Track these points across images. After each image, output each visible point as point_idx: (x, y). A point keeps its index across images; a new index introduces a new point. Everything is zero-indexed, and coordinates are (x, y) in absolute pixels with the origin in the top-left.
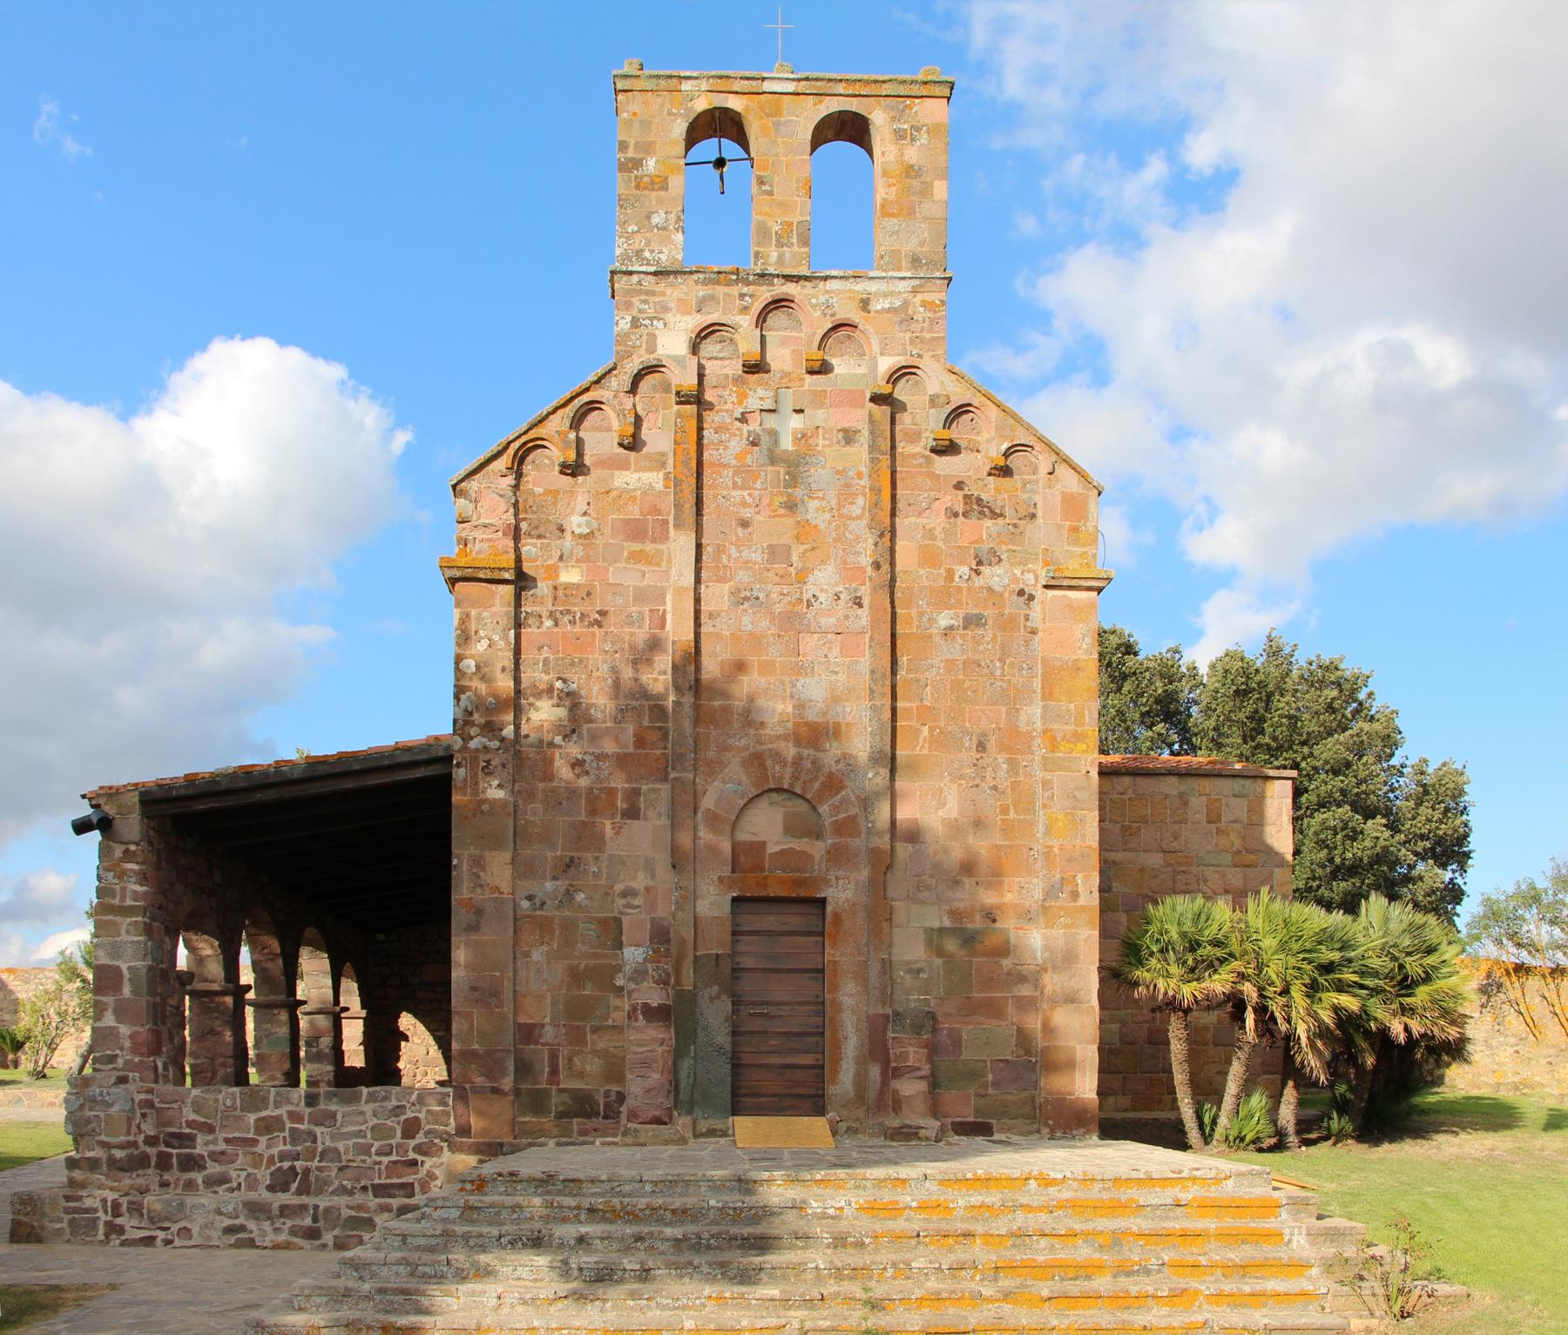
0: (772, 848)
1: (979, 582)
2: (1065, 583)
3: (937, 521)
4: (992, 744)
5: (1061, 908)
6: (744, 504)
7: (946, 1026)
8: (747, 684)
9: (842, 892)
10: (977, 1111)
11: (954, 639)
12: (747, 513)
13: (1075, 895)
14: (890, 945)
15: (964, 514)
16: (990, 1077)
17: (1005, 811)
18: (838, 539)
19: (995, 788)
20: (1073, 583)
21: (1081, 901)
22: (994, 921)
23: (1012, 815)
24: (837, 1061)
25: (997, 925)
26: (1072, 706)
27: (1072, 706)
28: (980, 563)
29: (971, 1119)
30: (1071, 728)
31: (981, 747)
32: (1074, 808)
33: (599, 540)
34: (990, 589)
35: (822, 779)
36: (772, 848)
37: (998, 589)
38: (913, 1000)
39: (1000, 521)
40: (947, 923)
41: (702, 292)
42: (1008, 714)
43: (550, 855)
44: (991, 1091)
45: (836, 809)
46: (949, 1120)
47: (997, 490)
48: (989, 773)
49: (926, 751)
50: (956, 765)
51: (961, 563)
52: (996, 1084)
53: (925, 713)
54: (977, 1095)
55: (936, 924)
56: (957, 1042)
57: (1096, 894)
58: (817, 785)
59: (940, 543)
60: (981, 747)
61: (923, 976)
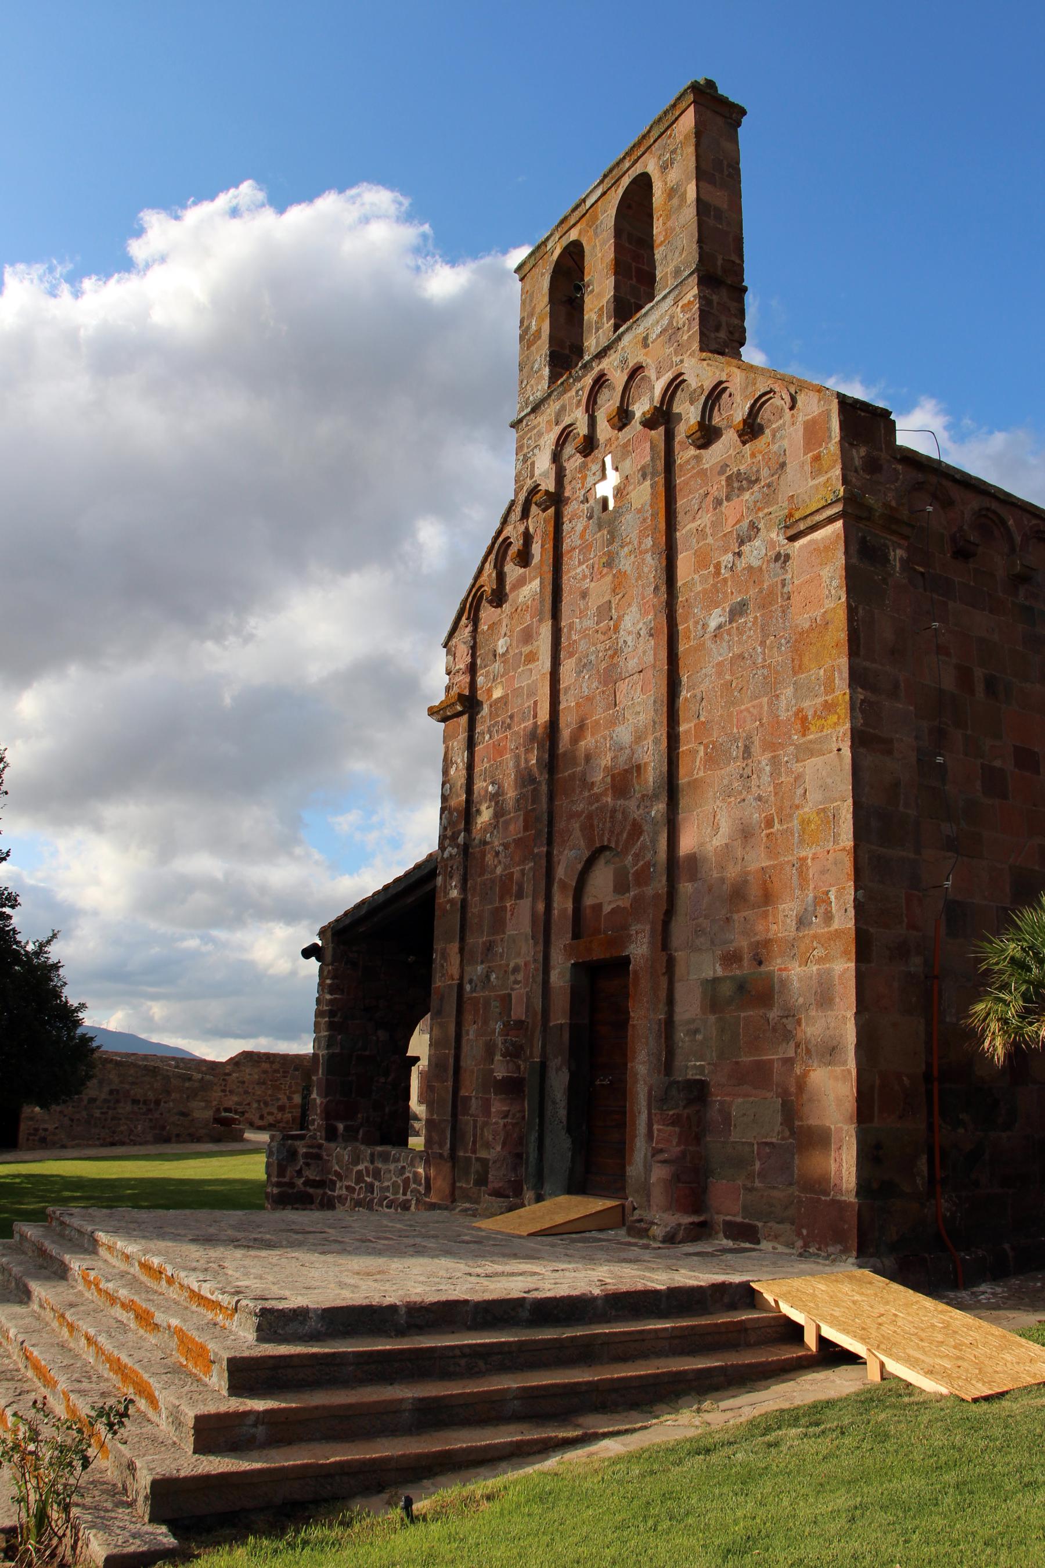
0: (607, 909)
2: (802, 526)
4: (756, 749)
5: (815, 937)
7: (717, 1098)
8: (588, 742)
9: (639, 949)
10: (745, 1208)
11: (722, 639)
13: (829, 918)
15: (728, 499)
16: (757, 1165)
17: (769, 823)
20: (809, 522)
22: (760, 963)
25: (763, 969)
28: (742, 543)
29: (739, 1219)
30: (820, 700)
34: (750, 568)
35: (628, 827)
36: (607, 909)
37: (756, 563)
39: (756, 488)
42: (770, 703)
43: (481, 941)
44: (757, 1184)
49: (701, 774)
50: (725, 782)
51: (726, 552)
52: (762, 1175)
53: (702, 728)
54: (745, 1188)
55: (709, 974)
56: (727, 1118)
57: (851, 912)
58: (625, 835)
59: (710, 540)
60: (747, 753)
61: (699, 1037)
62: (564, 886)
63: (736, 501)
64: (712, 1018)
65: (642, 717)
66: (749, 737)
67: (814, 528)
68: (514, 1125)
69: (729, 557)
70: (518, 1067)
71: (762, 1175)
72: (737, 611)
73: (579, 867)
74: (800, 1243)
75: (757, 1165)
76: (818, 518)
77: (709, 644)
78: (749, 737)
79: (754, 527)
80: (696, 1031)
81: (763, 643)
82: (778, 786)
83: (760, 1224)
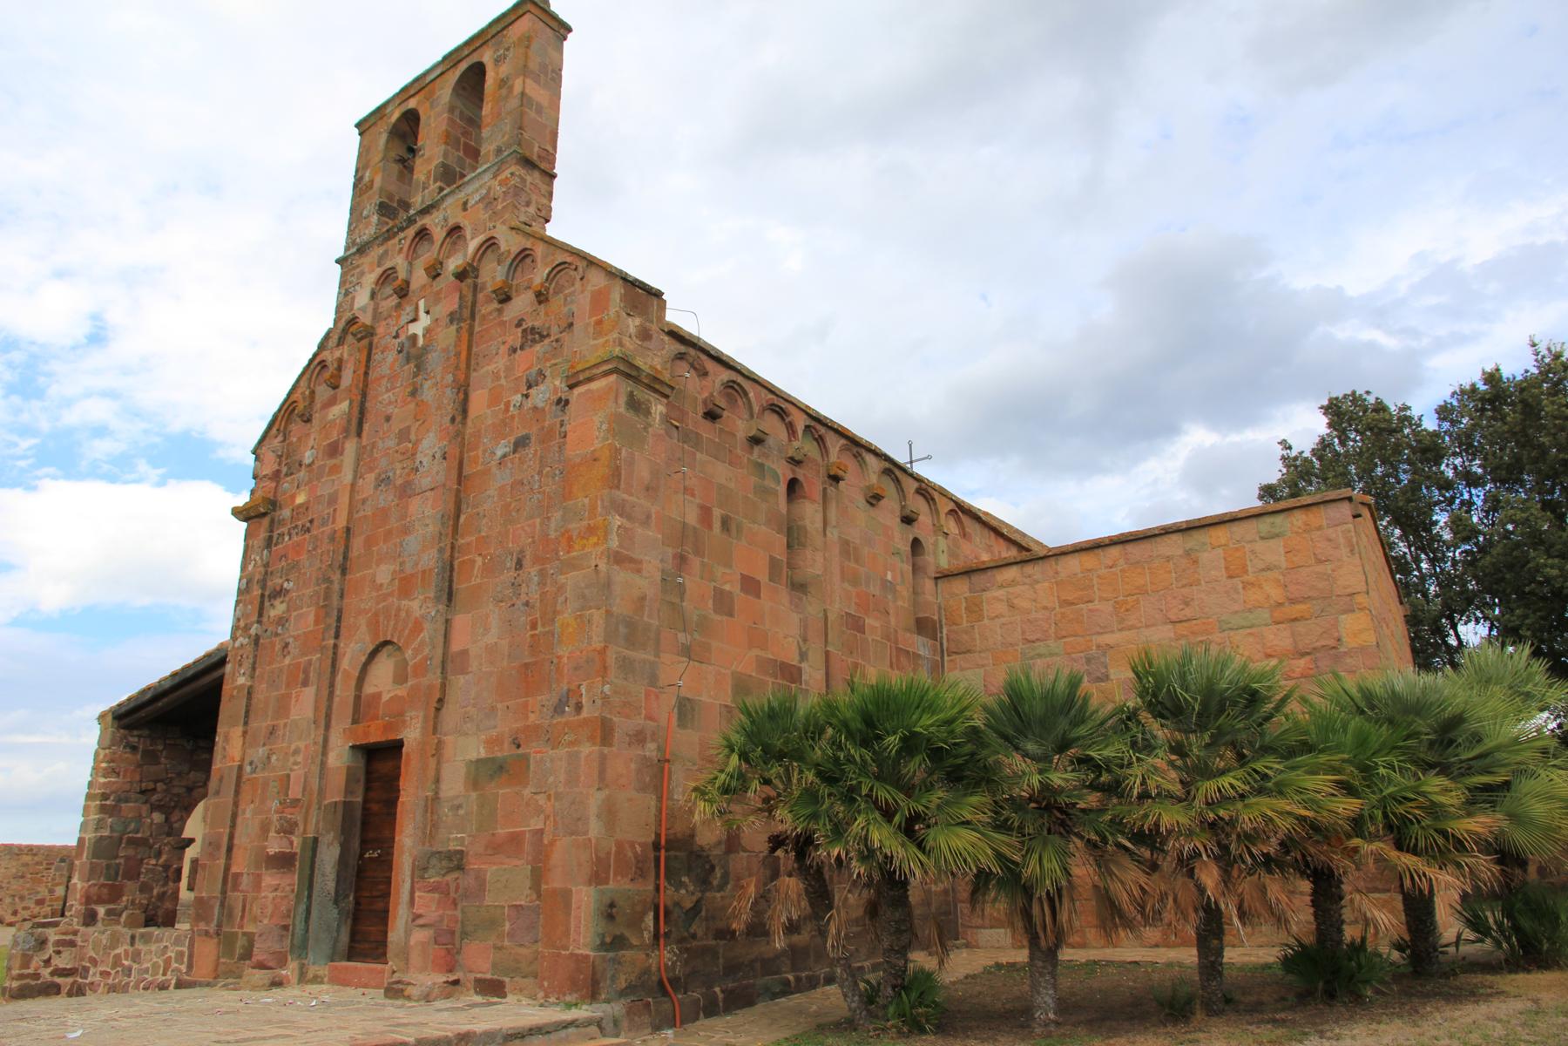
0: (386, 697)
1: (529, 404)
3: (500, 363)
4: (527, 562)
6: (390, 403)
7: (473, 865)
9: (412, 735)
10: (495, 966)
12: (390, 409)
13: (579, 707)
14: (437, 781)
16: (507, 926)
17: (534, 626)
18: (439, 408)
19: (527, 604)
20: (587, 374)
21: (585, 714)
23: (540, 629)
24: (397, 904)
26: (586, 501)
27: (586, 501)
28: (530, 387)
29: (489, 976)
30: (585, 523)
31: (519, 565)
32: (583, 609)
33: (318, 463)
34: (535, 408)
36: (386, 697)
37: (541, 405)
38: (453, 839)
39: (547, 341)
40: (483, 754)
41: (381, 250)
42: (542, 524)
45: (417, 651)
46: (472, 976)
47: (547, 314)
48: (524, 589)
51: (516, 392)
52: (511, 935)
54: (495, 947)
55: (473, 756)
59: (503, 382)
60: (519, 565)
61: (461, 812)
62: (347, 674)
63: (528, 350)
64: (474, 795)
65: (431, 528)
66: (522, 551)
67: (590, 380)
68: (283, 898)
69: (518, 397)
70: (291, 843)
71: (511, 935)
72: (521, 443)
73: (363, 659)
74: (541, 994)
75: (507, 926)
76: (596, 371)
77: (494, 470)
78: (522, 551)
79: (541, 373)
80: (459, 807)
81: (540, 473)
82: (543, 594)
83: (507, 980)
